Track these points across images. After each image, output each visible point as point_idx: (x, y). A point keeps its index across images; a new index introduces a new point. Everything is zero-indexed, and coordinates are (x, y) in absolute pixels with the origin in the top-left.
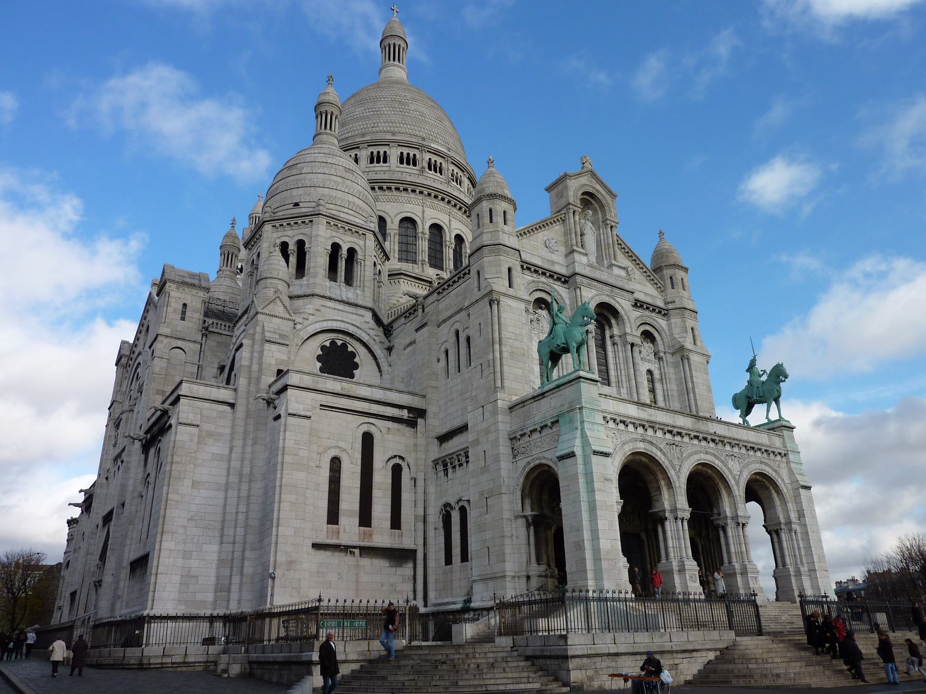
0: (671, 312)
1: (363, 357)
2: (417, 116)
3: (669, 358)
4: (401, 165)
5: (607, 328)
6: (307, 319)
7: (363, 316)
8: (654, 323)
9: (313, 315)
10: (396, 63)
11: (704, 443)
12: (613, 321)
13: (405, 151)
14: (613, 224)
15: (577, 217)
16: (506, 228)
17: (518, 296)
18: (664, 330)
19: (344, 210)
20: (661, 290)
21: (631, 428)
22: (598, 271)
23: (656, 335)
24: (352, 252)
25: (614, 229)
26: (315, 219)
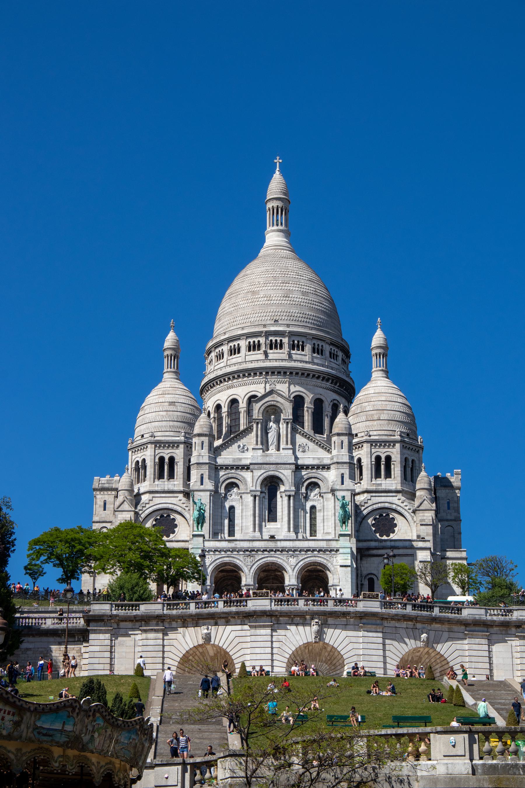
0: (332, 466)
1: (179, 521)
2: (264, 302)
3: (330, 495)
4: (250, 353)
6: (145, 507)
7: (177, 497)
8: (318, 476)
9: (148, 503)
11: (271, 553)
13: (251, 340)
15: (259, 425)
18: (325, 478)
19: (167, 434)
20: (329, 451)
21: (223, 553)
23: (320, 482)
24: (172, 460)
26: (149, 446)
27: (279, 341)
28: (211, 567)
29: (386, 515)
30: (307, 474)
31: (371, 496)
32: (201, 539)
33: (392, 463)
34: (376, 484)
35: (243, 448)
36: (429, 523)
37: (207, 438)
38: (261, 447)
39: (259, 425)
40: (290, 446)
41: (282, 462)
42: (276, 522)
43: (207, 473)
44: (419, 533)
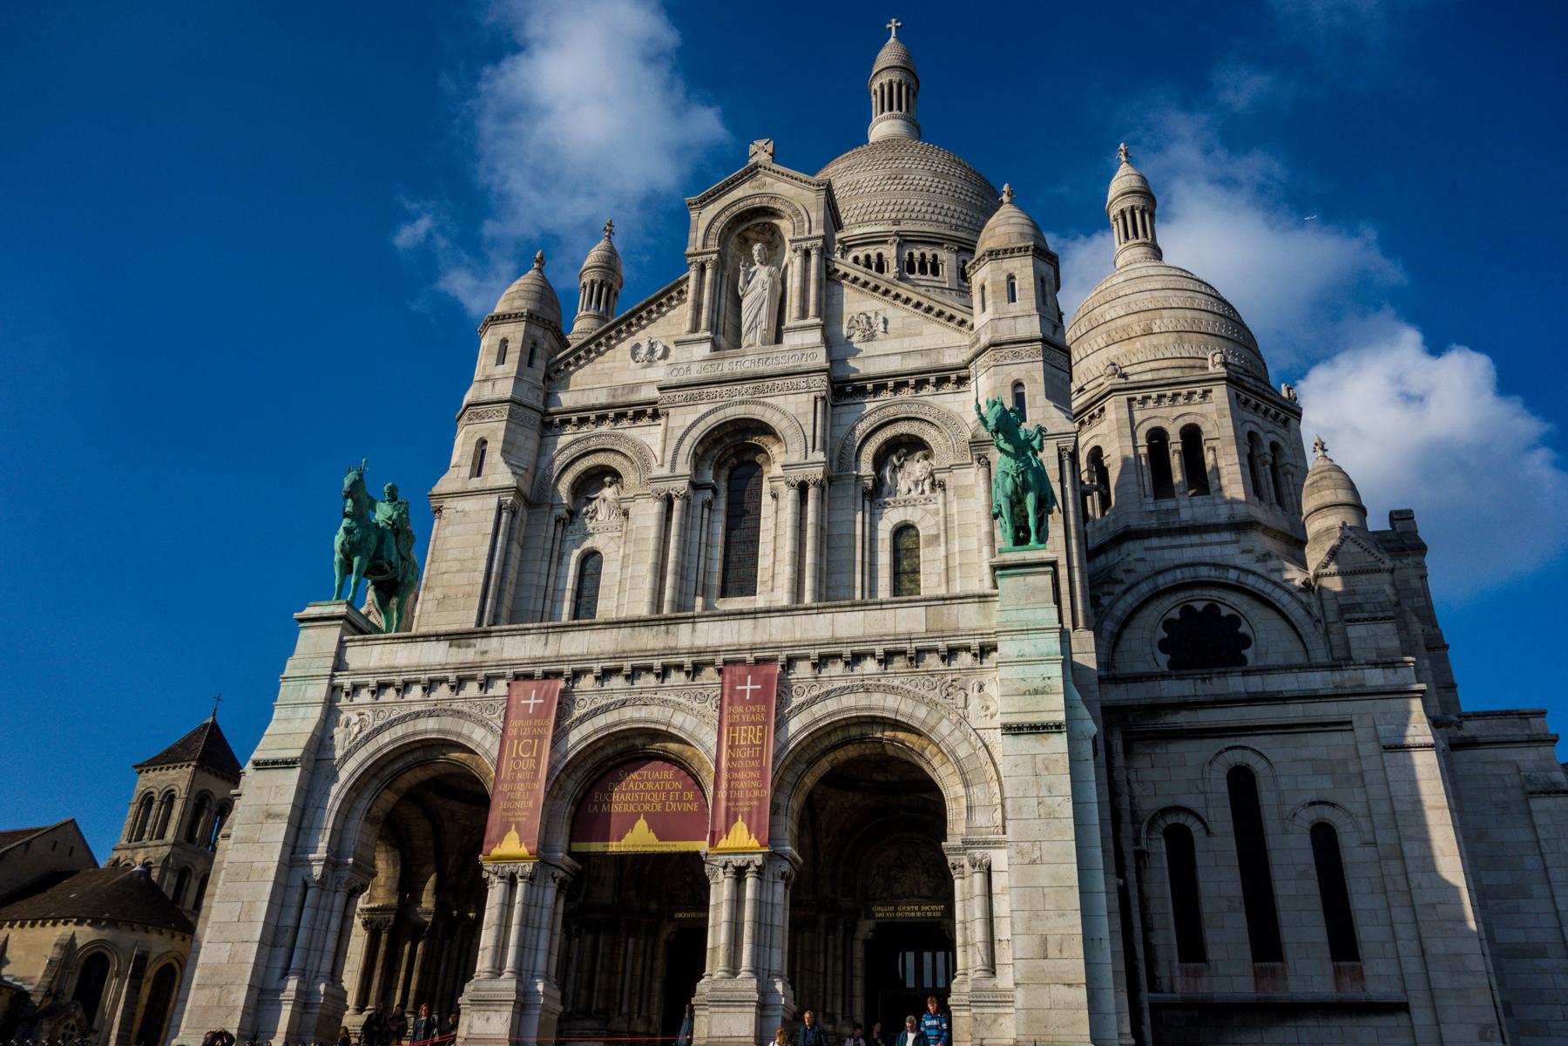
0: (972, 367)
5: (765, 468)
10: (886, 113)
12: (775, 450)
14: (805, 245)
16: (499, 370)
17: (488, 485)
22: (729, 361)
23: (929, 435)
25: (813, 252)
27: (874, 258)
28: (351, 765)
29: (1204, 608)
30: (880, 409)
31: (1146, 549)
32: (332, 634)
33: (1209, 444)
34: (1158, 512)
35: (652, 351)
36: (1380, 615)
37: (521, 327)
38: (708, 334)
39: (709, 273)
40: (811, 320)
41: (778, 371)
42: (755, 595)
43: (501, 435)
44: (1339, 653)
